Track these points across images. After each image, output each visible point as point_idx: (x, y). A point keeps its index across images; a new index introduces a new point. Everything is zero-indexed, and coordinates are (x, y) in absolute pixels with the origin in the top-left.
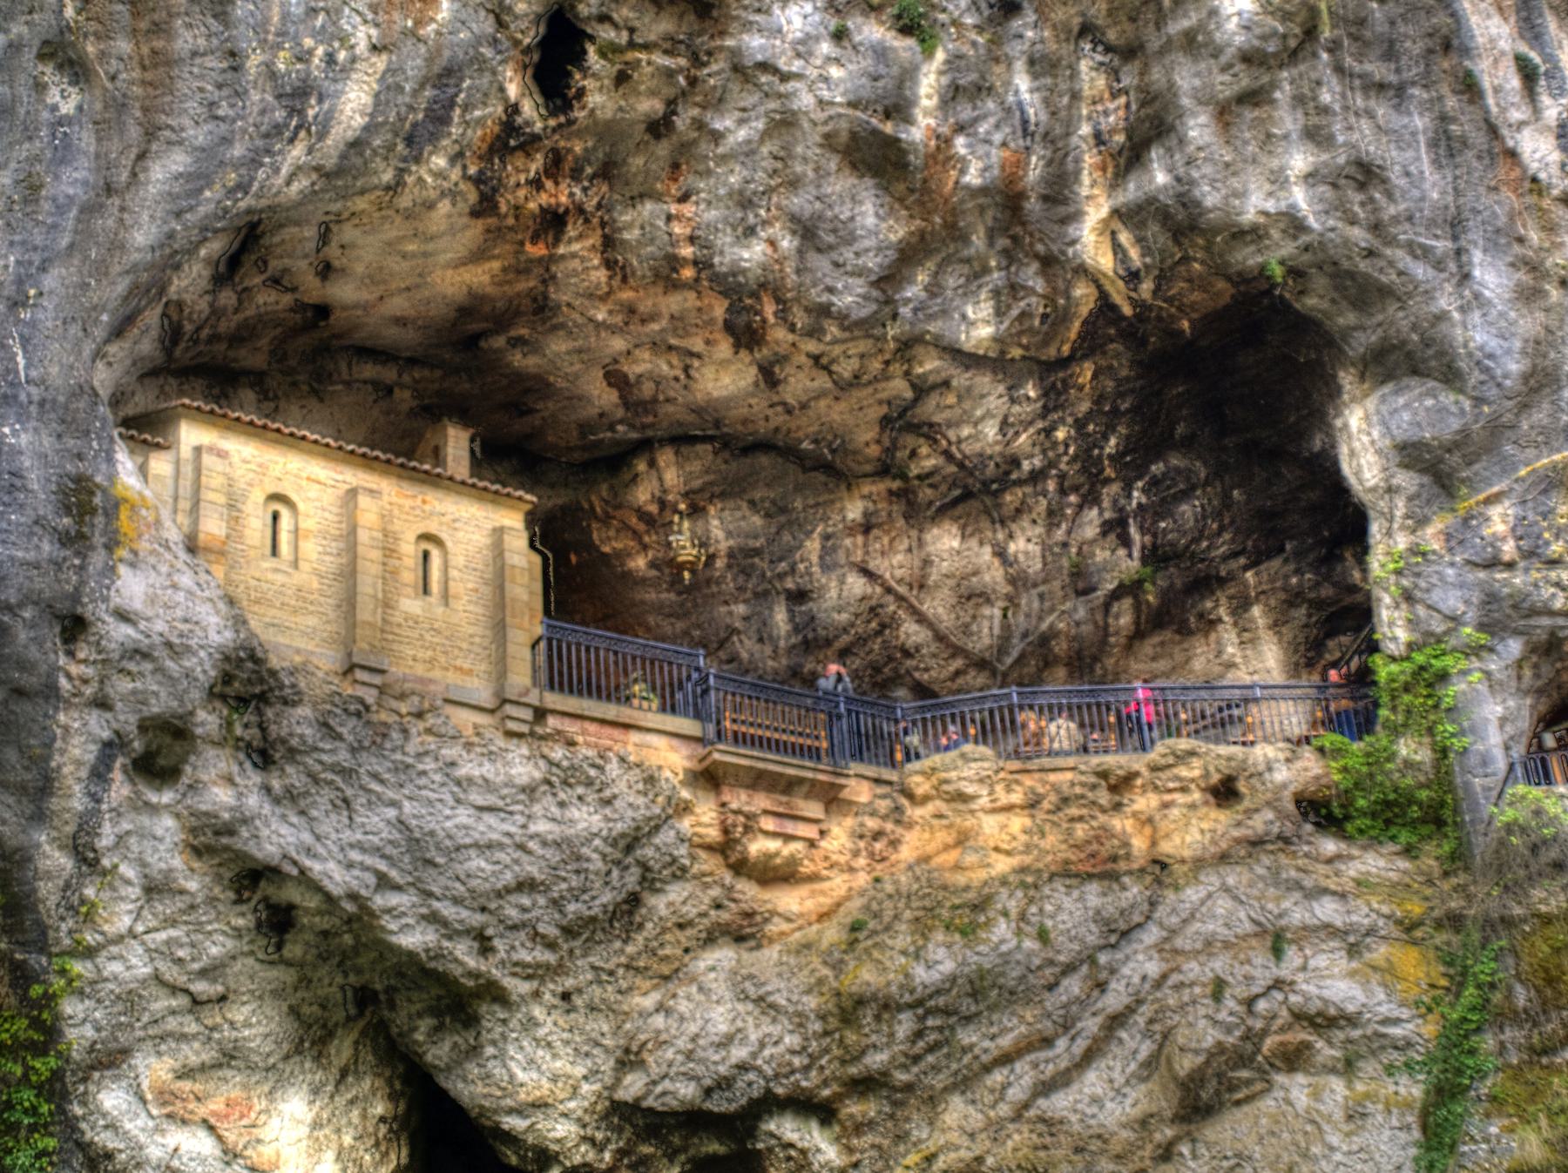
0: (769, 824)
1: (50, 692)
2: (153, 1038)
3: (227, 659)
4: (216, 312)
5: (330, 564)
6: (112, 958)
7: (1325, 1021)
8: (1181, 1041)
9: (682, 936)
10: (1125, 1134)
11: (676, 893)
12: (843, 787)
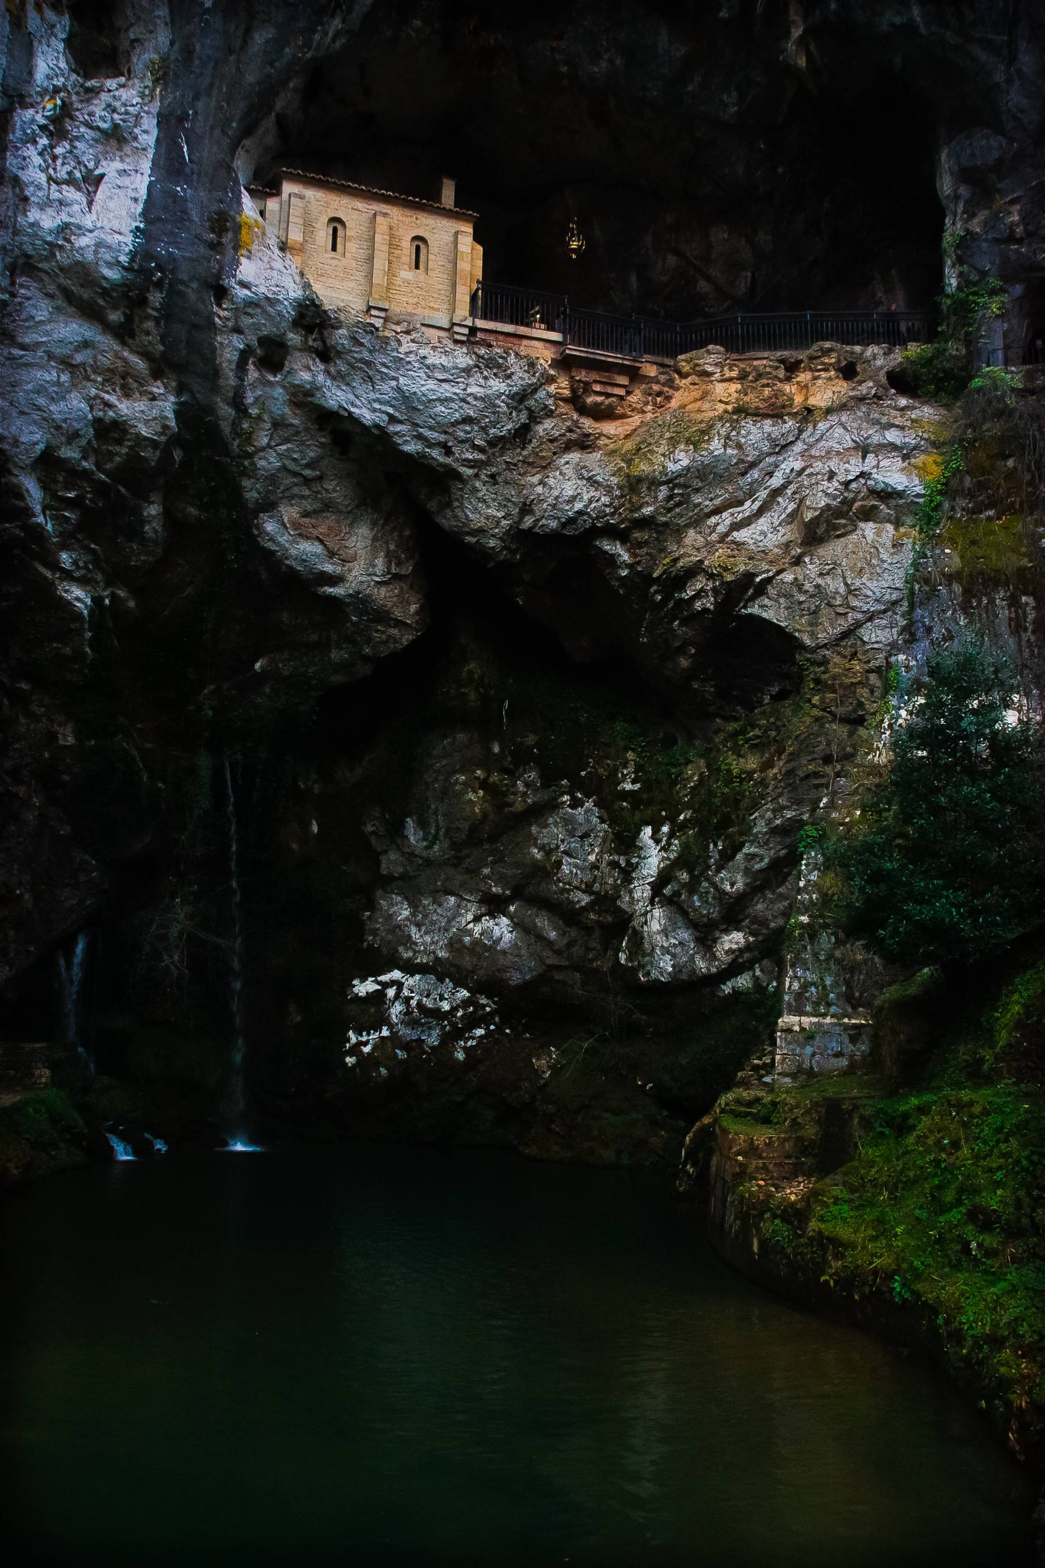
0: (597, 388)
2: (288, 497)
3: (300, 305)
5: (362, 254)
7: (887, 495)
8: (808, 503)
10: (776, 550)
11: (548, 424)
12: (640, 368)
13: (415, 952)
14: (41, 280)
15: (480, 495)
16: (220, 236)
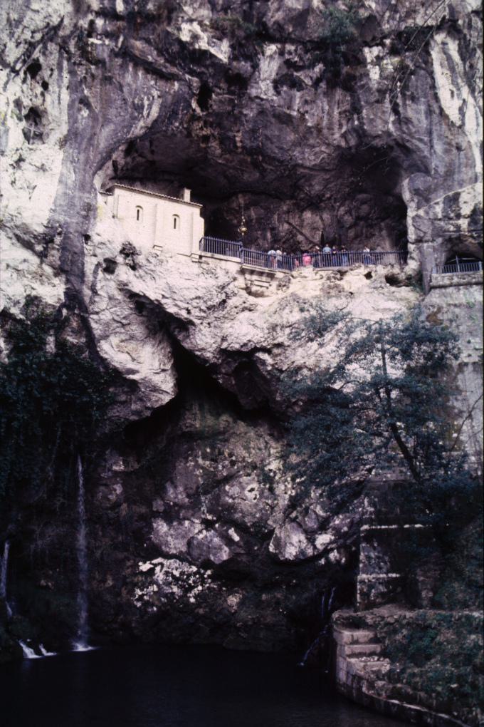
0: (256, 283)
1: (83, 254)
3: (123, 244)
4: (126, 163)
6: (103, 314)
9: (236, 310)
13: (170, 548)
14: (6, 231)
15: (202, 332)
16: (88, 213)
